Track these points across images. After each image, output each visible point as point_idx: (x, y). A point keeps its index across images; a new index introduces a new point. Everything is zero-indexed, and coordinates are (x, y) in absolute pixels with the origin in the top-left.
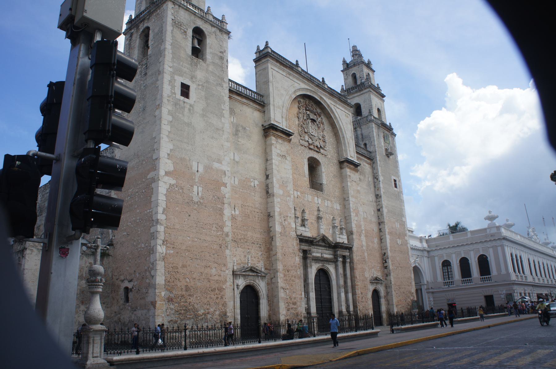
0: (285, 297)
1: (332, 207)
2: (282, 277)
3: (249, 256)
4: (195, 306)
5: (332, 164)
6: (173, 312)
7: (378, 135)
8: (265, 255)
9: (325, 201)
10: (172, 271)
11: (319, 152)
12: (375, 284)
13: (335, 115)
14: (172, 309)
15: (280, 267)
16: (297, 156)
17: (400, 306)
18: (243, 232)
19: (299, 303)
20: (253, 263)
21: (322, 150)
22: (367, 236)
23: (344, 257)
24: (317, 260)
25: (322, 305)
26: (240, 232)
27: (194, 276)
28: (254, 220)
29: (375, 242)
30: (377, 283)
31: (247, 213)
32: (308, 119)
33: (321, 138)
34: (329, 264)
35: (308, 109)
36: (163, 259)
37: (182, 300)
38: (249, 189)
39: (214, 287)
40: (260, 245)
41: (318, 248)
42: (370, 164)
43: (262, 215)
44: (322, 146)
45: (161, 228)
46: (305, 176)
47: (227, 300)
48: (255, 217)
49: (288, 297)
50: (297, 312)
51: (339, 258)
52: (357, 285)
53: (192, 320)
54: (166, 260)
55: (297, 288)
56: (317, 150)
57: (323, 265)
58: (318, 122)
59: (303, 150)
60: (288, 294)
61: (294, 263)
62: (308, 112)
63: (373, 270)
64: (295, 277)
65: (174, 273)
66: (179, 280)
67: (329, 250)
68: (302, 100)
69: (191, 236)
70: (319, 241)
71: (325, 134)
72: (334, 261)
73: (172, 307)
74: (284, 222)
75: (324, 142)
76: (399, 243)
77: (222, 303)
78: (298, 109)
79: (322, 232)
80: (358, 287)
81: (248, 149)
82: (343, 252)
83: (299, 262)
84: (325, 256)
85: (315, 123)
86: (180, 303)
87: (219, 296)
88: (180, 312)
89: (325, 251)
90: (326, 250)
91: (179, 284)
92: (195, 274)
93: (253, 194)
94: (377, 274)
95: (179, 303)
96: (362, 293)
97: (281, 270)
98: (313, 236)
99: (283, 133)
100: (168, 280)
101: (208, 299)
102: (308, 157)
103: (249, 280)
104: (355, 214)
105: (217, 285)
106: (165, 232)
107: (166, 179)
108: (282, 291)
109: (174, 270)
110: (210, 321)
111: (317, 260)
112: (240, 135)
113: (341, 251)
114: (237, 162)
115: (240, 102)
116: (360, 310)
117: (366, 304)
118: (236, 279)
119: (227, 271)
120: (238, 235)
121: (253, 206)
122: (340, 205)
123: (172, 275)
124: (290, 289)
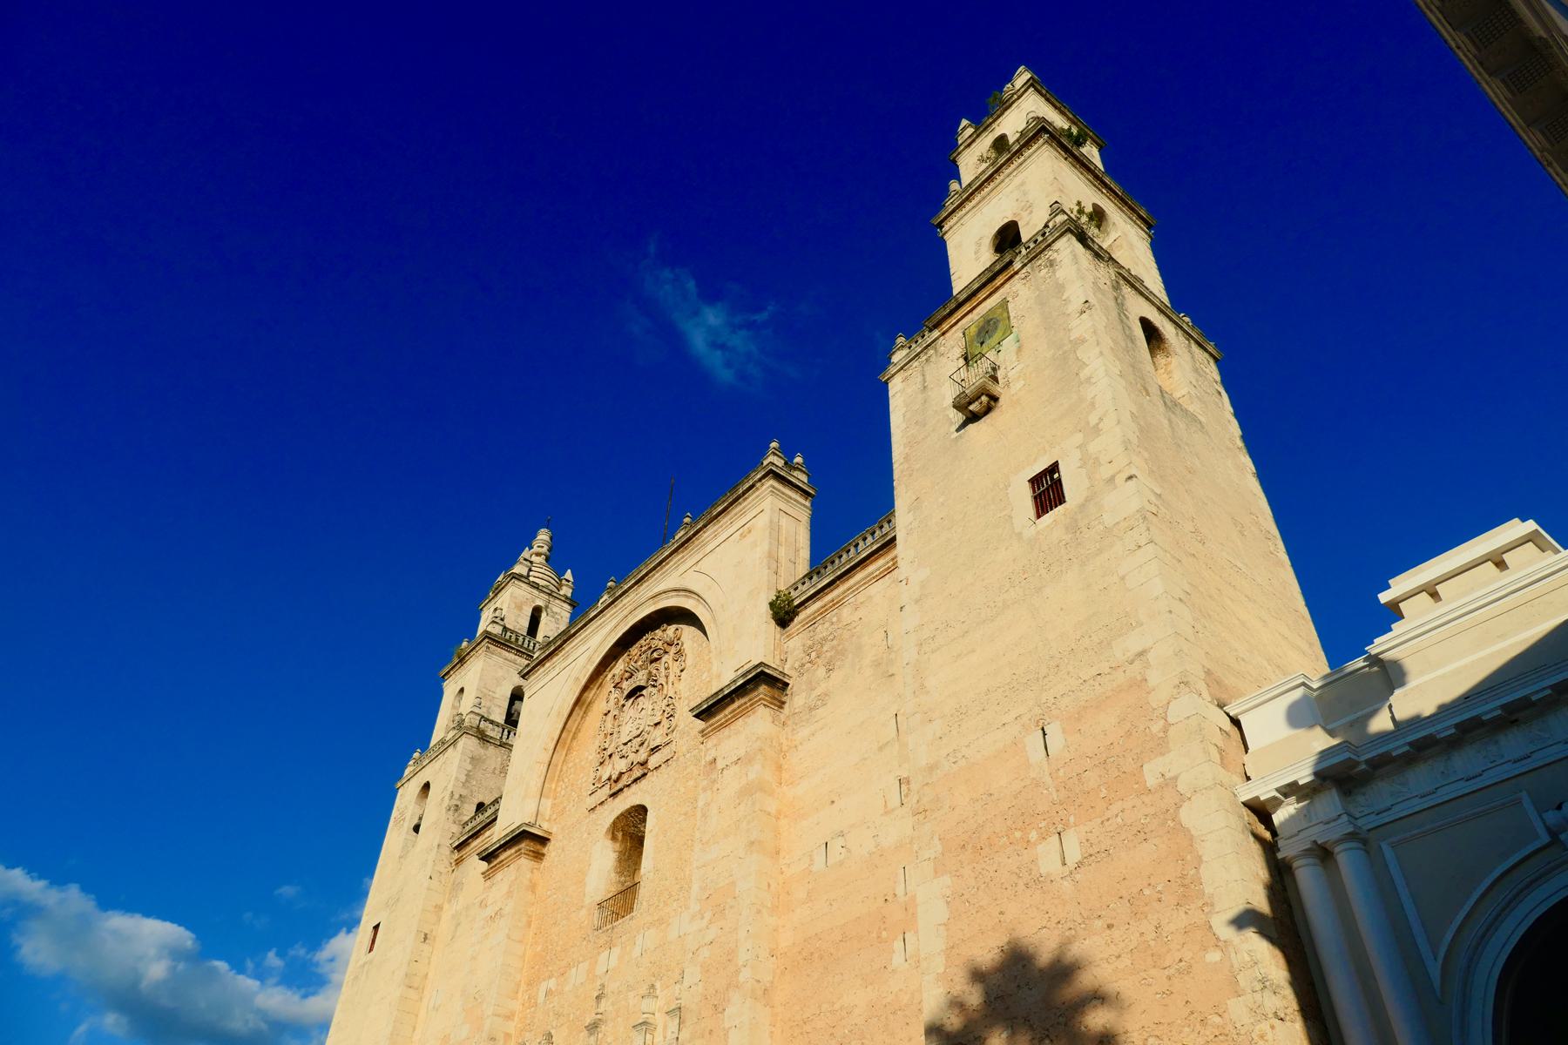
11: (644, 775)
29: (898, 959)
76: (1048, 862)
85: (644, 692)
99: (510, 848)
102: (605, 830)
104: (708, 915)
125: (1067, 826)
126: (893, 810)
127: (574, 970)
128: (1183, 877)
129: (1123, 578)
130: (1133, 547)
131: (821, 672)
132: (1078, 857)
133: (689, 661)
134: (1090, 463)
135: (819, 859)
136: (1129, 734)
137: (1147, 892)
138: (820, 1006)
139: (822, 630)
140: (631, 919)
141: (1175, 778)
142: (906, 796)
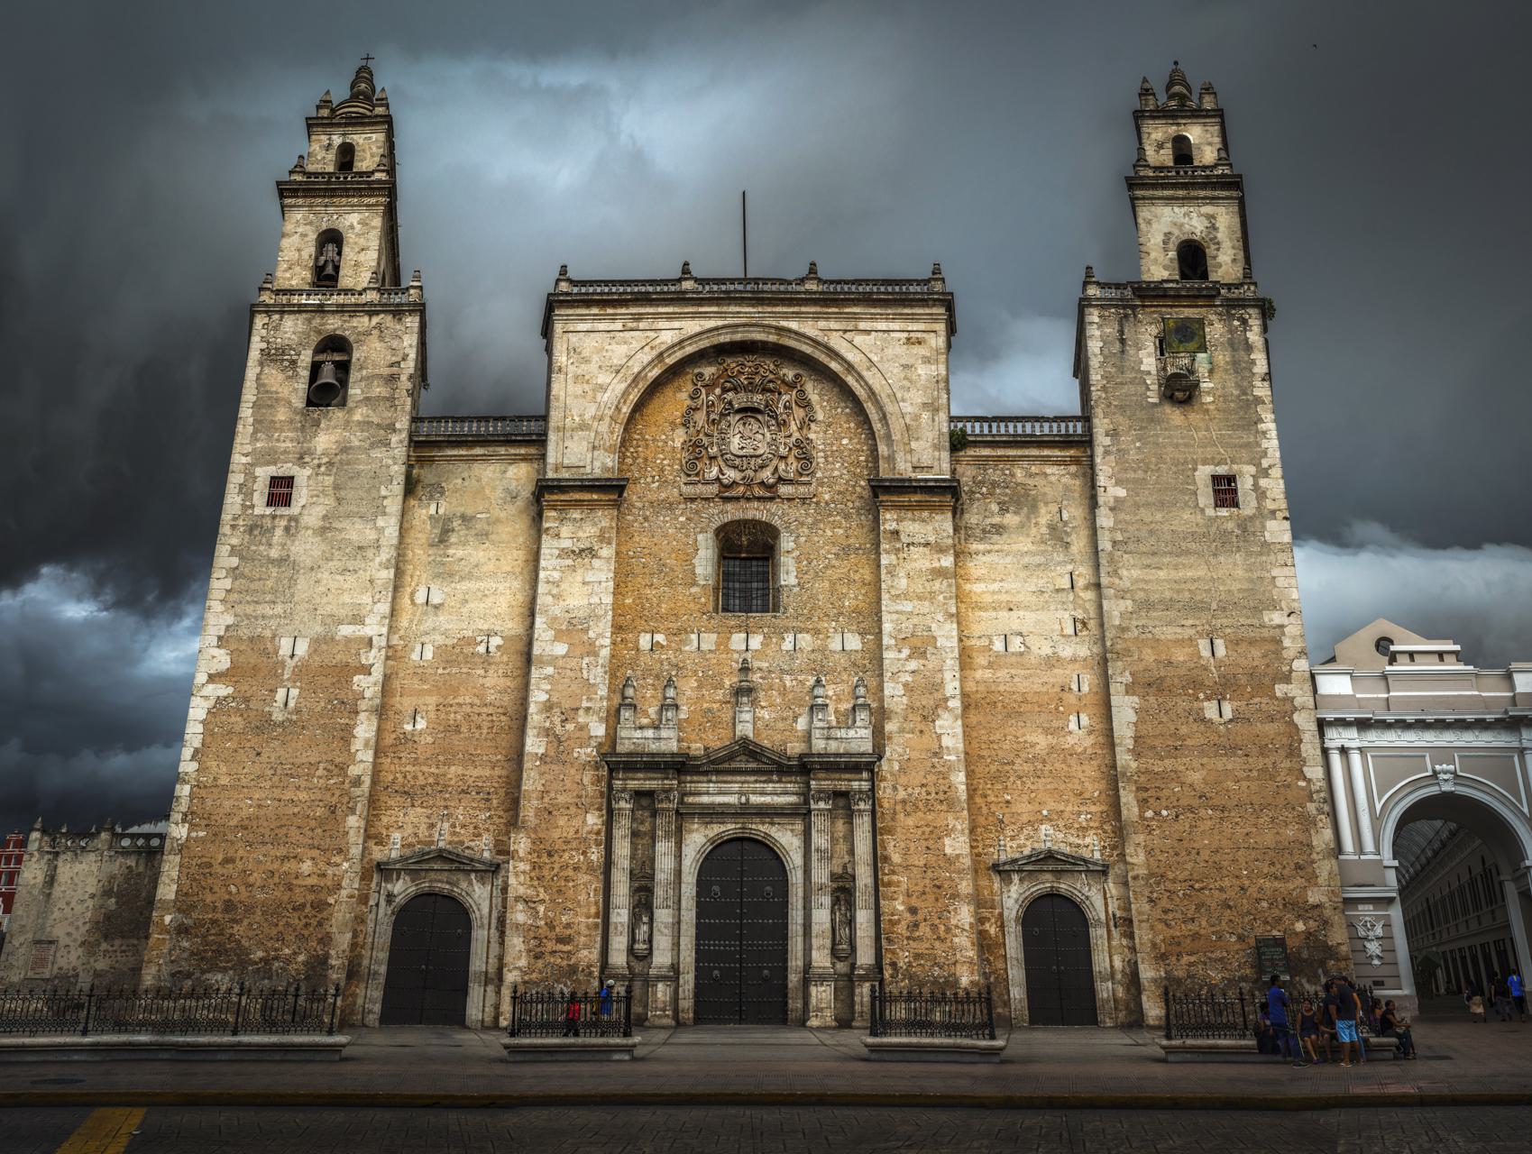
0: (530, 922)
1: (823, 650)
2: (524, 872)
3: (446, 825)
4: (243, 942)
5: (838, 518)
6: (185, 955)
7: (1123, 341)
8: (500, 817)
9: (785, 635)
10: (198, 874)
11: (771, 499)
12: (1049, 876)
13: (846, 361)
14: (184, 950)
15: (521, 844)
16: (665, 536)
17: (1192, 959)
18: (433, 770)
19: (583, 939)
20: (457, 839)
21: (784, 490)
22: (1020, 714)
23: (842, 798)
24: (711, 814)
25: (741, 946)
26: (425, 769)
27: (251, 879)
28: (477, 735)
29: (1073, 726)
30: (1058, 873)
31: (452, 722)
32: (729, 414)
33: (783, 451)
34: (772, 824)
35: (728, 385)
36: (180, 851)
37: (213, 931)
38: (467, 662)
39: (302, 900)
40: (489, 793)
41: (729, 778)
42: (1075, 461)
43: (503, 718)
44: (783, 474)
45: (183, 791)
46: (694, 584)
47: (334, 929)
48: (479, 727)
49: (543, 923)
50: (571, 963)
51: (812, 801)
52: (889, 884)
53: (231, 972)
54: (185, 850)
55: (582, 897)
56: (758, 492)
57: (744, 828)
58: (781, 410)
59: (697, 512)
60: (541, 914)
61: (577, 832)
62: (730, 396)
63: (1045, 828)
64: (575, 869)
65: (202, 877)
66: (211, 889)
67: (780, 781)
68: (709, 371)
69: (257, 796)
70: (731, 757)
71: (812, 436)
72: (801, 813)
73: (186, 944)
74: (559, 727)
75: (805, 458)
77: (320, 936)
78: (689, 402)
79: (745, 729)
80: (892, 889)
81: (477, 566)
82: (839, 780)
83: (596, 828)
84: (755, 799)
85: (760, 417)
86: (206, 936)
87: (314, 922)
88: (203, 954)
89: (758, 785)
90: (764, 782)
91: (209, 898)
92: (255, 875)
93: (482, 672)
94: (1072, 839)
95: (204, 937)
96: (913, 911)
97: (521, 854)
98: (706, 749)
100: (185, 890)
101: (280, 928)
102: (714, 526)
103: (430, 881)
105: (310, 897)
106: (192, 796)
107: (210, 690)
108: (520, 906)
109: (201, 870)
110: (278, 974)
111: (711, 814)
112: (453, 539)
113: (825, 779)
114: (436, 607)
115: (461, 459)
116: (894, 965)
117: (937, 944)
118: (387, 881)
119: (345, 864)
120: (415, 777)
121: (477, 702)
122: (862, 634)
123: (195, 880)
124: (553, 901)
125: (1224, 698)
126: (1070, 636)
127: (694, 637)
128: (1291, 745)
129: (1274, 578)
130: (1283, 562)
131: (994, 507)
132: (1231, 717)
133: (820, 416)
134: (1261, 494)
135: (998, 646)
136: (1267, 665)
137: (1270, 746)
138: (1005, 736)
139: (993, 474)
140: (775, 617)
141: (1293, 698)
142: (1081, 631)
